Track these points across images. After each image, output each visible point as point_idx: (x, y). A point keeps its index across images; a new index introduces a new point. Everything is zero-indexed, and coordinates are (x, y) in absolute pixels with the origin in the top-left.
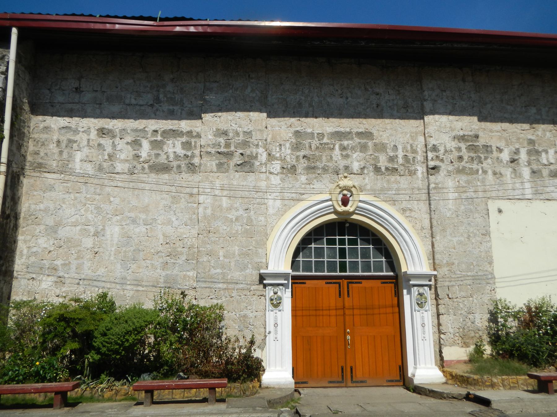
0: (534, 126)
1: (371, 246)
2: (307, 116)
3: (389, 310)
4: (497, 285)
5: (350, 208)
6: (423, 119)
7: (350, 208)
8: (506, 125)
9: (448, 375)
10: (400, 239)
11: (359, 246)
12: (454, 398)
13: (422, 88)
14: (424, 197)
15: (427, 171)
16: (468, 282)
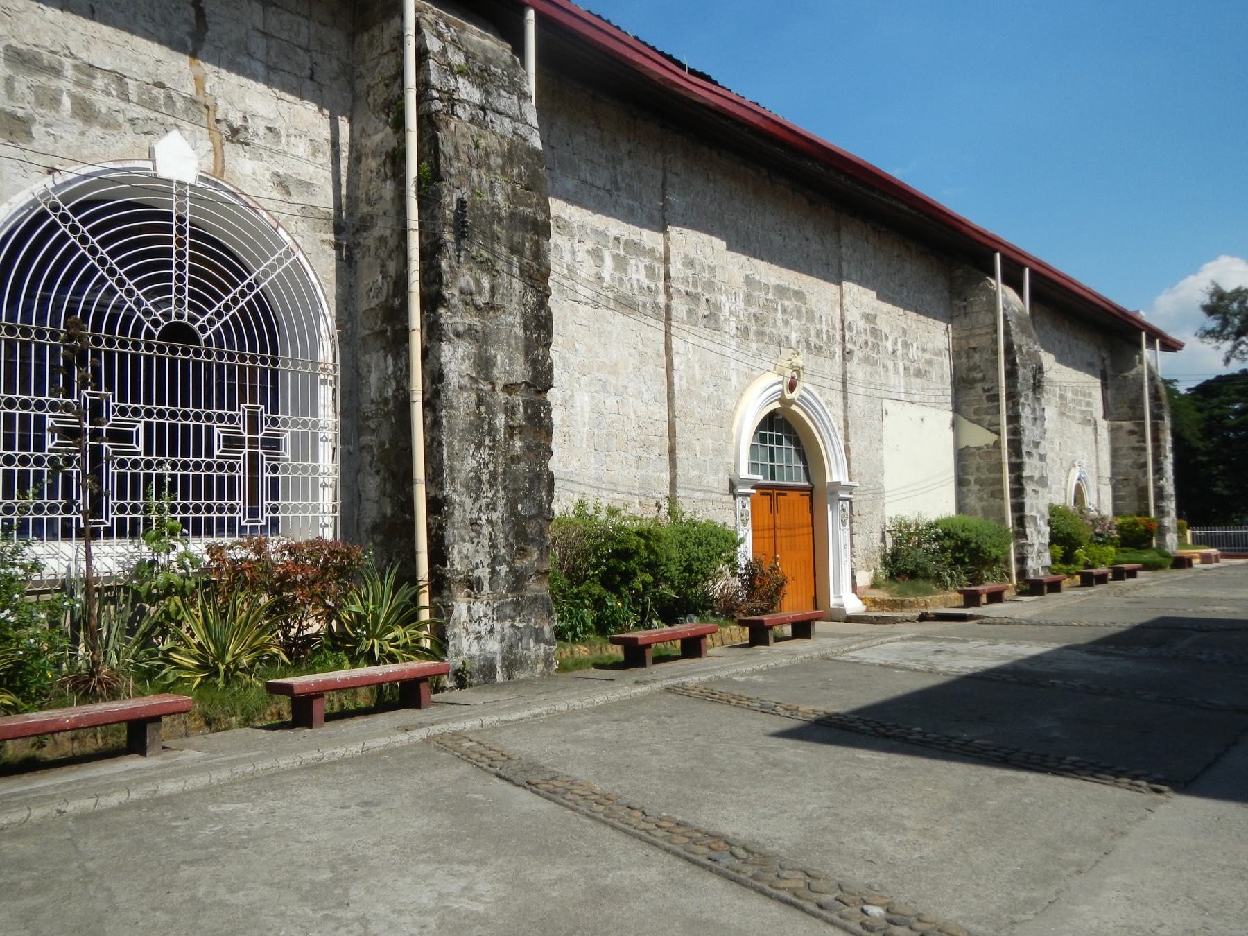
0: (907, 312)
1: (792, 447)
2: (755, 257)
3: (766, 534)
4: (885, 501)
5: (794, 395)
6: (840, 284)
7: (794, 395)
8: (890, 306)
9: (868, 602)
10: (827, 441)
11: (784, 446)
12: (908, 621)
13: (839, 241)
14: (839, 386)
15: (843, 355)
16: (871, 496)
